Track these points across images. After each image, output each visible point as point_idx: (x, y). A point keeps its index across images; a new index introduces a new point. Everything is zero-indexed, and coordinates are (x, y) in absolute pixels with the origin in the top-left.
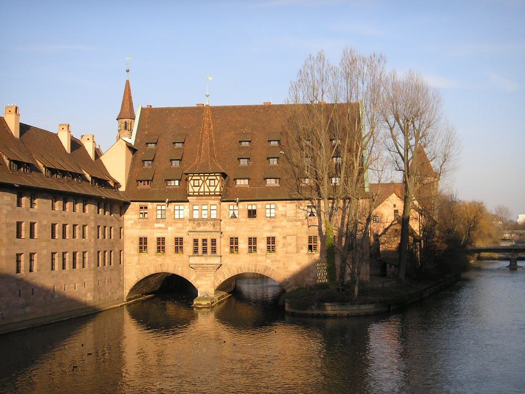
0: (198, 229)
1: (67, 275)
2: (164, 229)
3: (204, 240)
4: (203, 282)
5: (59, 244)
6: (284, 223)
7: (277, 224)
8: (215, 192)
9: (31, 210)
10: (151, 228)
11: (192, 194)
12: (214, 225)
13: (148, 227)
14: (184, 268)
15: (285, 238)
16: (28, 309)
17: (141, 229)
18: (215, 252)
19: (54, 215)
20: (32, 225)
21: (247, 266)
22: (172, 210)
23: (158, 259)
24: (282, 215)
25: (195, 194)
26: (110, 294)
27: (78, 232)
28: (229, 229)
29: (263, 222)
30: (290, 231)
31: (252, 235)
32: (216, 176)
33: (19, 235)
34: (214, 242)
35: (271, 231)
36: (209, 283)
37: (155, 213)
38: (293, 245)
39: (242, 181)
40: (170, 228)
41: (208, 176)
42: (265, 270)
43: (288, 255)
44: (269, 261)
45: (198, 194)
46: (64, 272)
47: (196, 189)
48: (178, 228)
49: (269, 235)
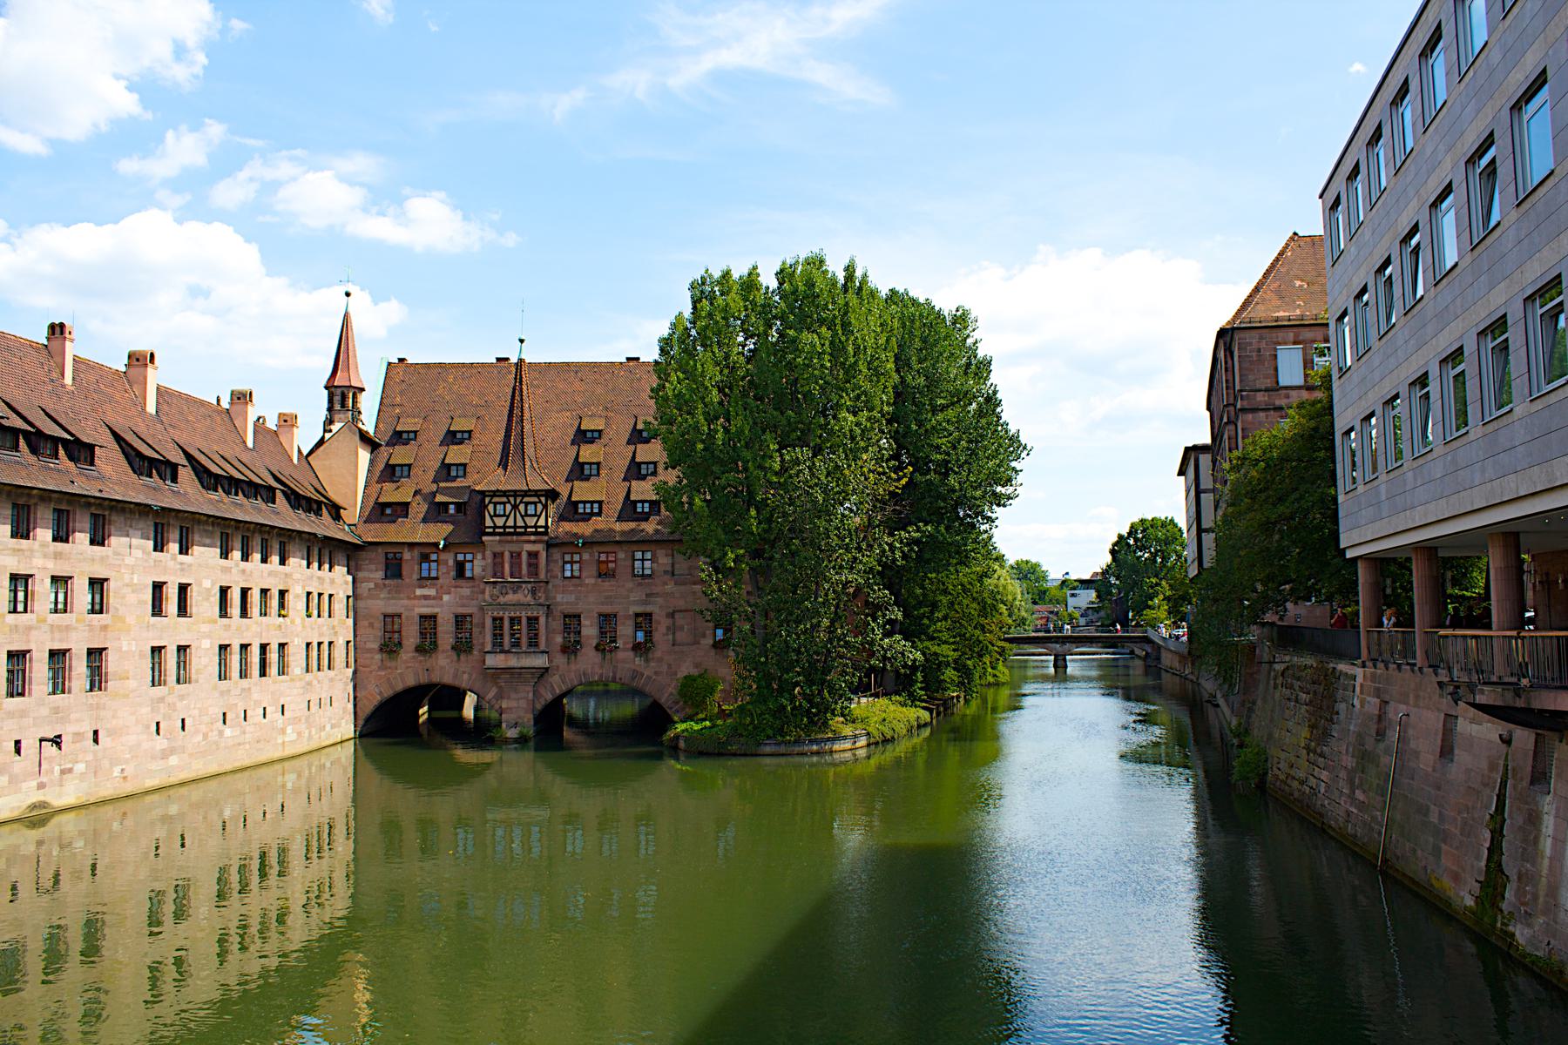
0: (502, 600)
4: (513, 704)
5: (238, 630)
6: (670, 587)
8: (536, 526)
10: (409, 598)
12: (533, 592)
15: (672, 615)
16: (173, 760)
18: (537, 645)
19: (226, 570)
20: (183, 589)
22: (451, 562)
26: (328, 727)
27: (275, 603)
28: (565, 600)
29: (630, 585)
30: (681, 604)
31: (607, 609)
33: (157, 609)
34: (533, 621)
35: (645, 603)
36: (523, 704)
37: (416, 568)
40: (446, 598)
43: (677, 648)
47: (500, 522)
48: (462, 597)
49: (639, 609)
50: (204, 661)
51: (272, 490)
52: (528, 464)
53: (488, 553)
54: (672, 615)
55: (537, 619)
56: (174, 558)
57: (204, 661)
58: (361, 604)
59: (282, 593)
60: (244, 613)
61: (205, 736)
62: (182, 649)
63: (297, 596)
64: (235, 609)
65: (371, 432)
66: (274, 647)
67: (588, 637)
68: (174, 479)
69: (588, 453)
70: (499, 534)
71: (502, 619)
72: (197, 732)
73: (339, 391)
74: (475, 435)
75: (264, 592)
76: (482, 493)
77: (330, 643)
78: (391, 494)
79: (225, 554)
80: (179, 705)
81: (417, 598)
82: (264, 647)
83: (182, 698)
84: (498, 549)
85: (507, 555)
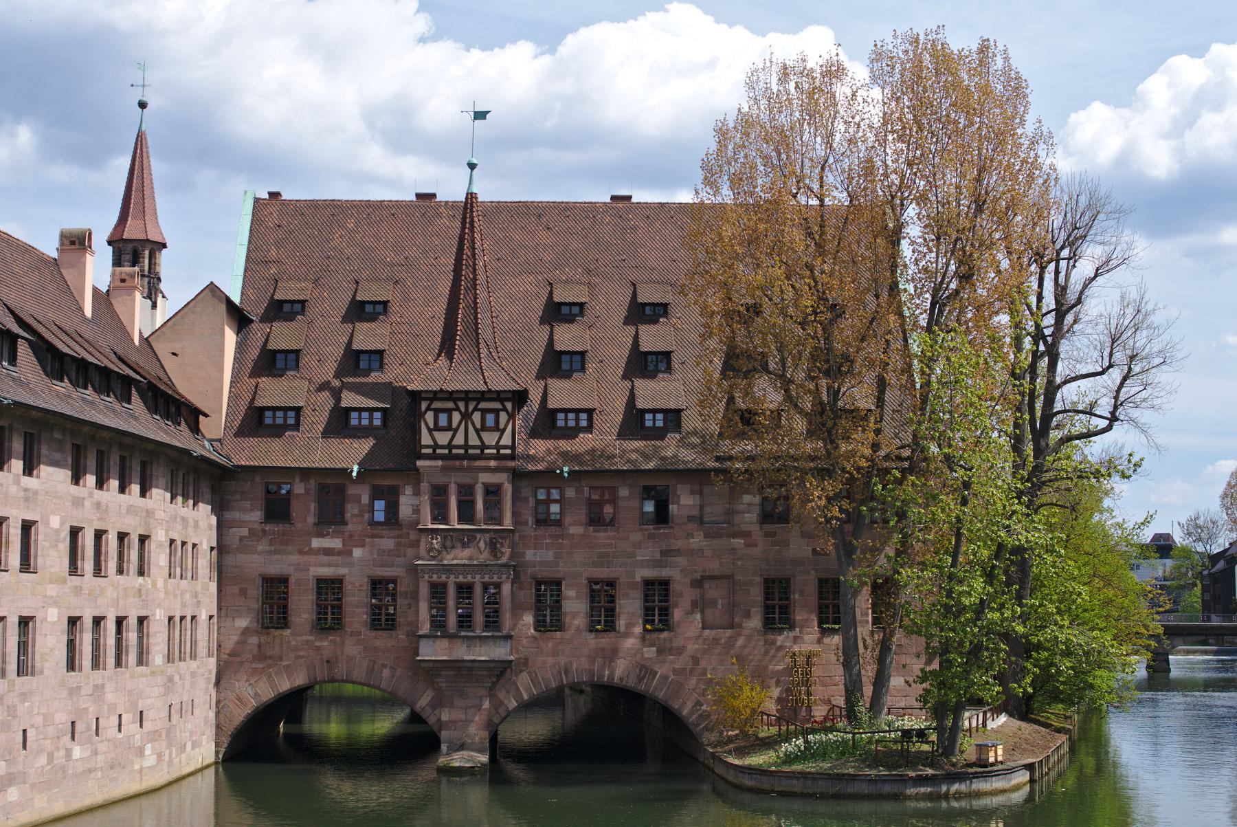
1: (99, 688)
2: (339, 553)
3: (465, 590)
6: (697, 541)
7: (679, 544)
8: (498, 447)
9: (26, 481)
10: (301, 552)
11: (430, 451)
12: (493, 547)
13: (290, 548)
14: (399, 672)
15: (698, 583)
17: (270, 553)
21: (584, 663)
22: (365, 499)
23: (318, 644)
24: (691, 518)
25: (438, 451)
27: (133, 555)
28: (539, 557)
29: (636, 537)
30: (714, 566)
31: (603, 573)
32: (502, 401)
35: (659, 564)
38: (720, 601)
39: (571, 416)
40: (357, 552)
41: (479, 400)
42: (640, 679)
44: (650, 652)
45: (446, 451)
46: (97, 677)
47: (443, 438)
48: (381, 552)
49: (650, 573)
50: (50, 643)
51: (127, 382)
52: (484, 351)
53: (425, 486)
54: (698, 583)
55: (498, 586)
56: (17, 482)
57: (50, 643)
58: (229, 560)
59: (143, 539)
60: (98, 571)
61: (51, 757)
62: (24, 622)
63: (160, 545)
64: (88, 565)
65: (236, 299)
66: (133, 622)
67: (575, 615)
68: (13, 360)
69: (567, 337)
70: (442, 457)
71: (445, 585)
72: (40, 751)
73: (129, 247)
74: (394, 308)
75: (122, 537)
76: (416, 396)
77: (193, 618)
78: (274, 392)
79: (76, 480)
80: (22, 708)
81: (311, 552)
82: (120, 621)
83: (24, 696)
84: (440, 480)
85: (453, 489)
